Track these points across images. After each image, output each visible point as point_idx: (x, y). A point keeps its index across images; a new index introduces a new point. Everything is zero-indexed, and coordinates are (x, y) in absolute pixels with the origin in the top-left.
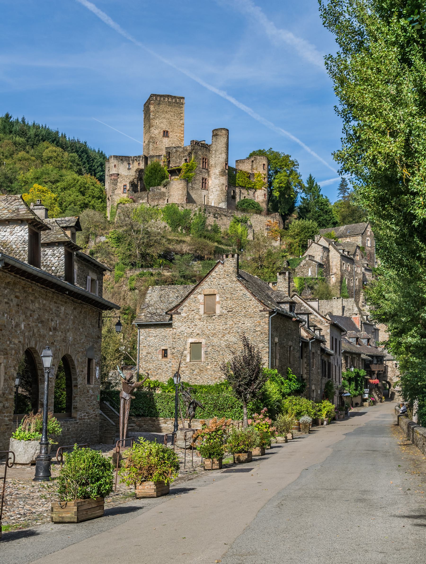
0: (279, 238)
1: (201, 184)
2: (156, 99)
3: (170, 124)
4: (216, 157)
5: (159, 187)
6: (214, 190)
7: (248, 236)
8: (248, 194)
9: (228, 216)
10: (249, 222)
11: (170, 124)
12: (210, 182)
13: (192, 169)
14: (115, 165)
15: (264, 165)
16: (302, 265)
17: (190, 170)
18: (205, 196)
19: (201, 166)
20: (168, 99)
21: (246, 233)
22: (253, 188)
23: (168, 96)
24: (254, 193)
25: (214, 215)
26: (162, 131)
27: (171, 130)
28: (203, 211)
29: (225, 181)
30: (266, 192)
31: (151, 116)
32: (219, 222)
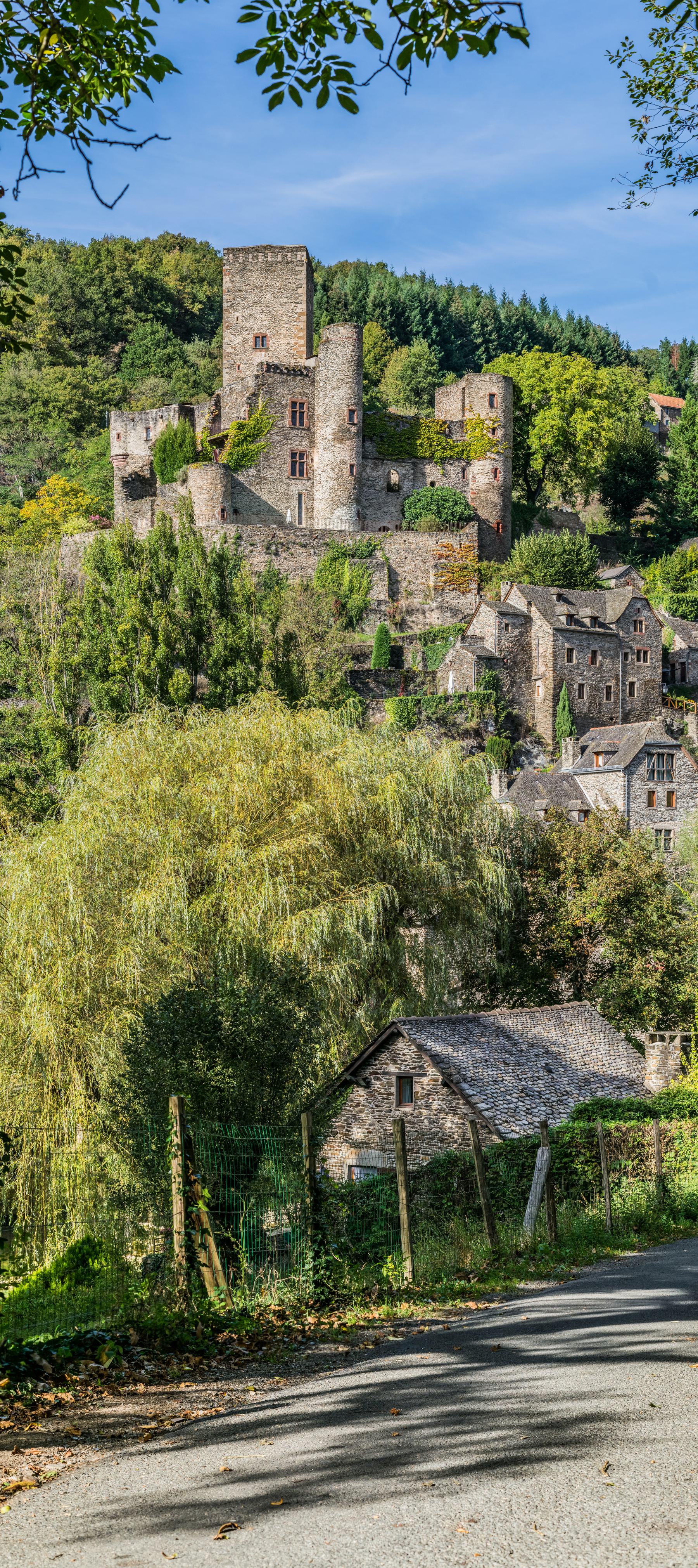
0: (474, 586)
1: (287, 467)
2: (236, 259)
3: (272, 316)
4: (325, 396)
5: (174, 485)
6: (323, 478)
7: (370, 589)
8: (444, 475)
9: (313, 547)
10: (379, 554)
11: (272, 316)
12: (316, 460)
13: (258, 435)
14: (119, 436)
15: (492, 396)
16: (447, 661)
17: (255, 436)
18: (300, 495)
19: (287, 422)
20: (266, 255)
21: (364, 583)
22: (458, 459)
23: (265, 249)
24: (463, 470)
25: (268, 548)
26: (251, 335)
27: (274, 331)
28: (231, 541)
29: (347, 453)
30: (499, 465)
31: (225, 304)
32: (281, 565)
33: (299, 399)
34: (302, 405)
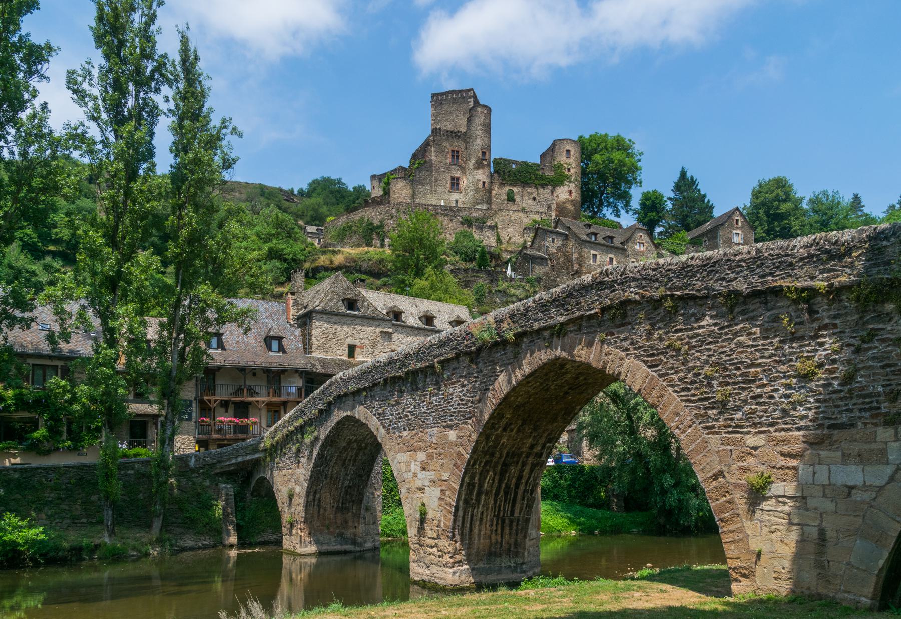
1: (449, 185)
2: (437, 99)
19: (449, 161)
33: (456, 149)
34: (458, 152)
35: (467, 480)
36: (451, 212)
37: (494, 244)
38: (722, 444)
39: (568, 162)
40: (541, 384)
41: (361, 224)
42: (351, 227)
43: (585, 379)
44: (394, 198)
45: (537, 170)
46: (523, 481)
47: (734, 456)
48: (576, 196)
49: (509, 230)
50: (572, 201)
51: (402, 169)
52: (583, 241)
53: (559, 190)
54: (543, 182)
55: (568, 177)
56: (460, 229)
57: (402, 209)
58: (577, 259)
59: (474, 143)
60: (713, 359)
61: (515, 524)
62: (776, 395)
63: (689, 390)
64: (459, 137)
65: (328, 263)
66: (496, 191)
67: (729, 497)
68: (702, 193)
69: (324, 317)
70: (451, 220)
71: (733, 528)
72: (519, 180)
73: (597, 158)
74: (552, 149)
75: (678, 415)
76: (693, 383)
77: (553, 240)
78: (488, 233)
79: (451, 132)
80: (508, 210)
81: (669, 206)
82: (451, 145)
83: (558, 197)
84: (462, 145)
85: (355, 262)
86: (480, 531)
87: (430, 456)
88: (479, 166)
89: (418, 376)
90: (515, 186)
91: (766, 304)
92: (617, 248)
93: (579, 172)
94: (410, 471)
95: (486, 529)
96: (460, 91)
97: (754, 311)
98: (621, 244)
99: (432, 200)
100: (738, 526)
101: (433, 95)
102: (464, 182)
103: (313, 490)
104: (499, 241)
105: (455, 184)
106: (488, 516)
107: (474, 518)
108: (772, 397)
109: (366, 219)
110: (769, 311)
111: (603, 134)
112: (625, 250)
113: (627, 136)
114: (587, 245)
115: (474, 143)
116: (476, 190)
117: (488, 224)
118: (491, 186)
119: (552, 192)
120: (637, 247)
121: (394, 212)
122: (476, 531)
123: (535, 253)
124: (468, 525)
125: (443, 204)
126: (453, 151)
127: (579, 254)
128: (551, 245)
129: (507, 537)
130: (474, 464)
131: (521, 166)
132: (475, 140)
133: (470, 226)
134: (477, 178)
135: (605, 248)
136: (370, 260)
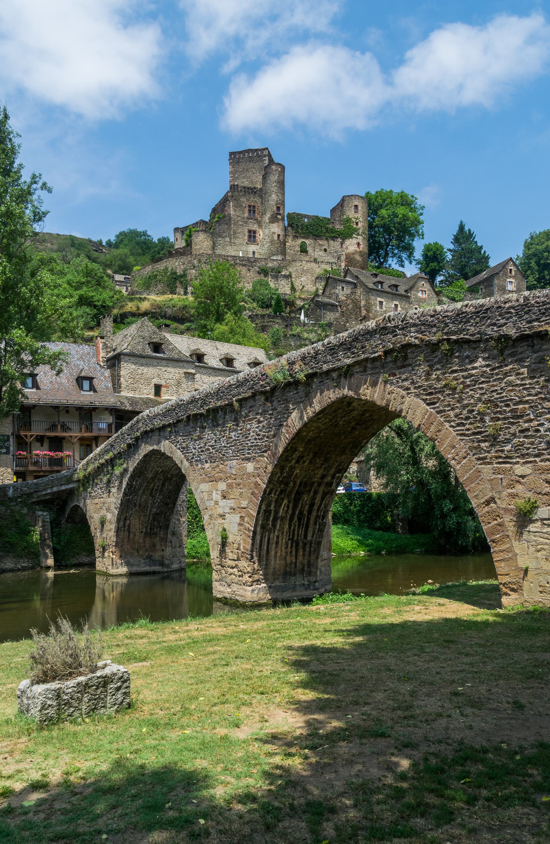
1: (246, 238)
2: (235, 157)
12: (261, 235)
19: (246, 215)
34: (254, 207)
35: (263, 507)
36: (249, 262)
37: (288, 292)
38: (494, 473)
39: (356, 216)
40: (331, 420)
41: (166, 273)
42: (156, 275)
43: (371, 415)
44: (196, 249)
45: (328, 224)
46: (315, 508)
47: (504, 484)
48: (364, 247)
49: (302, 279)
50: (360, 252)
51: (203, 222)
52: (370, 289)
53: (348, 242)
54: (333, 235)
55: (356, 230)
56: (257, 278)
57: (204, 259)
58: (365, 306)
59: (270, 198)
60: (486, 396)
61: (308, 546)
62: (541, 429)
63: (464, 425)
64: (255, 193)
65: (134, 309)
66: (290, 242)
67: (499, 520)
68: (479, 244)
69: (132, 358)
70: (249, 270)
71: (503, 547)
72: (311, 233)
73: (383, 212)
74: (342, 204)
75: (454, 447)
76: (467, 418)
77: (343, 288)
78: (283, 282)
79: (248, 188)
80: (302, 261)
81: (449, 256)
82: (248, 200)
83: (347, 248)
84: (258, 200)
85: (160, 308)
86: (276, 553)
87: (230, 486)
88: (274, 219)
89: (218, 413)
90: (307, 238)
91: (533, 346)
92: (401, 295)
93: (366, 225)
94: (212, 499)
95: (281, 551)
96: (256, 150)
97: (521, 353)
98: (405, 291)
99: (231, 251)
100: (508, 546)
101: (231, 154)
102: (261, 234)
103: (123, 517)
104: (293, 289)
105: (252, 236)
106: (283, 540)
107: (271, 541)
108: (538, 431)
109: (170, 269)
110: (535, 353)
111: (388, 190)
112: (408, 297)
113: (409, 192)
114: (374, 292)
115: (270, 198)
116: (272, 242)
117: (283, 273)
118: (286, 238)
119: (342, 244)
120: (420, 294)
121: (196, 262)
122: (273, 553)
123: (326, 300)
124: (265, 548)
125: (241, 255)
126: (250, 206)
127: (366, 301)
128: (341, 292)
129: (300, 558)
130: (270, 493)
131: (313, 220)
132: (270, 195)
133: (266, 275)
134: (272, 231)
135: (390, 295)
136: (174, 307)
